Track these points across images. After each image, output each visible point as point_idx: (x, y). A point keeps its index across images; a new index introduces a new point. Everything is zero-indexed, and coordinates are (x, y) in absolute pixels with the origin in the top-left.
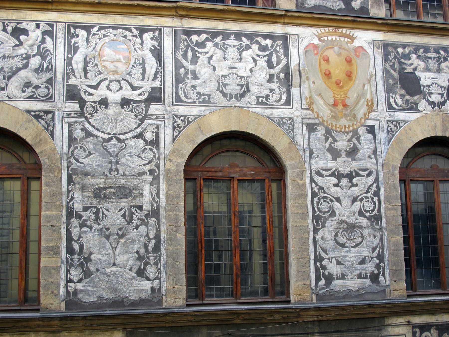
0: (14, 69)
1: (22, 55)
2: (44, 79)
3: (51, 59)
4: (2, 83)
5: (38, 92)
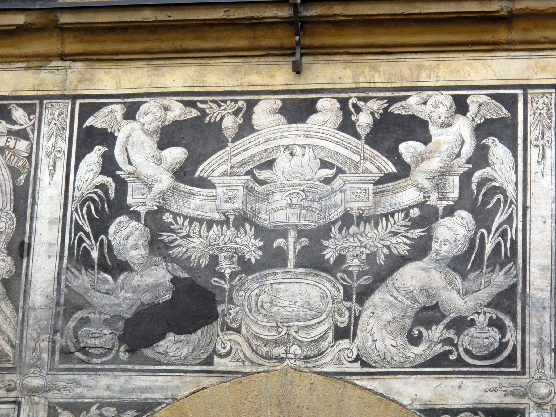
0: (381, 260)
1: (406, 211)
2: (486, 294)
3: (509, 220)
4: (341, 314)
5: (464, 341)
